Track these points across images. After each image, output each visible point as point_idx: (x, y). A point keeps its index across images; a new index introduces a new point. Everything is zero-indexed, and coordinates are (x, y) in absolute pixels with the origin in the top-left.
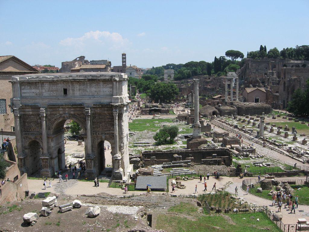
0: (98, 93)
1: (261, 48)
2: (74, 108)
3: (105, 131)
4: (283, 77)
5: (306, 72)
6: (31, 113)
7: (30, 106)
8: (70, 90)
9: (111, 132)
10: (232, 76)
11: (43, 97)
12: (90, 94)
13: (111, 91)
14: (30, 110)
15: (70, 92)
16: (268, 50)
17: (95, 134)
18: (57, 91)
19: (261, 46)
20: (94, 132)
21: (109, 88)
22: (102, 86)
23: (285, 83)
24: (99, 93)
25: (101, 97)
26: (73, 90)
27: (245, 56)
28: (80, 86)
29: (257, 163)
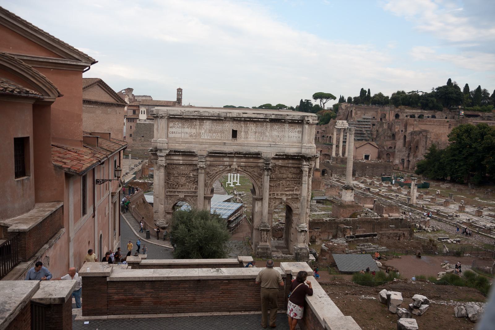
0: (281, 139)
1: (363, 92)
2: (245, 157)
3: (286, 191)
4: (404, 130)
6: (181, 162)
7: (182, 152)
8: (241, 132)
9: (295, 192)
10: (343, 125)
11: (201, 141)
12: (270, 140)
13: (299, 137)
14: (180, 158)
15: (241, 135)
16: (372, 95)
17: (272, 195)
18: (222, 132)
19: (362, 89)
20: (271, 193)
22: (287, 129)
23: (405, 137)
24: (282, 139)
25: (286, 144)
26: (246, 133)
27: (337, 101)
28: (256, 127)
29: (443, 239)
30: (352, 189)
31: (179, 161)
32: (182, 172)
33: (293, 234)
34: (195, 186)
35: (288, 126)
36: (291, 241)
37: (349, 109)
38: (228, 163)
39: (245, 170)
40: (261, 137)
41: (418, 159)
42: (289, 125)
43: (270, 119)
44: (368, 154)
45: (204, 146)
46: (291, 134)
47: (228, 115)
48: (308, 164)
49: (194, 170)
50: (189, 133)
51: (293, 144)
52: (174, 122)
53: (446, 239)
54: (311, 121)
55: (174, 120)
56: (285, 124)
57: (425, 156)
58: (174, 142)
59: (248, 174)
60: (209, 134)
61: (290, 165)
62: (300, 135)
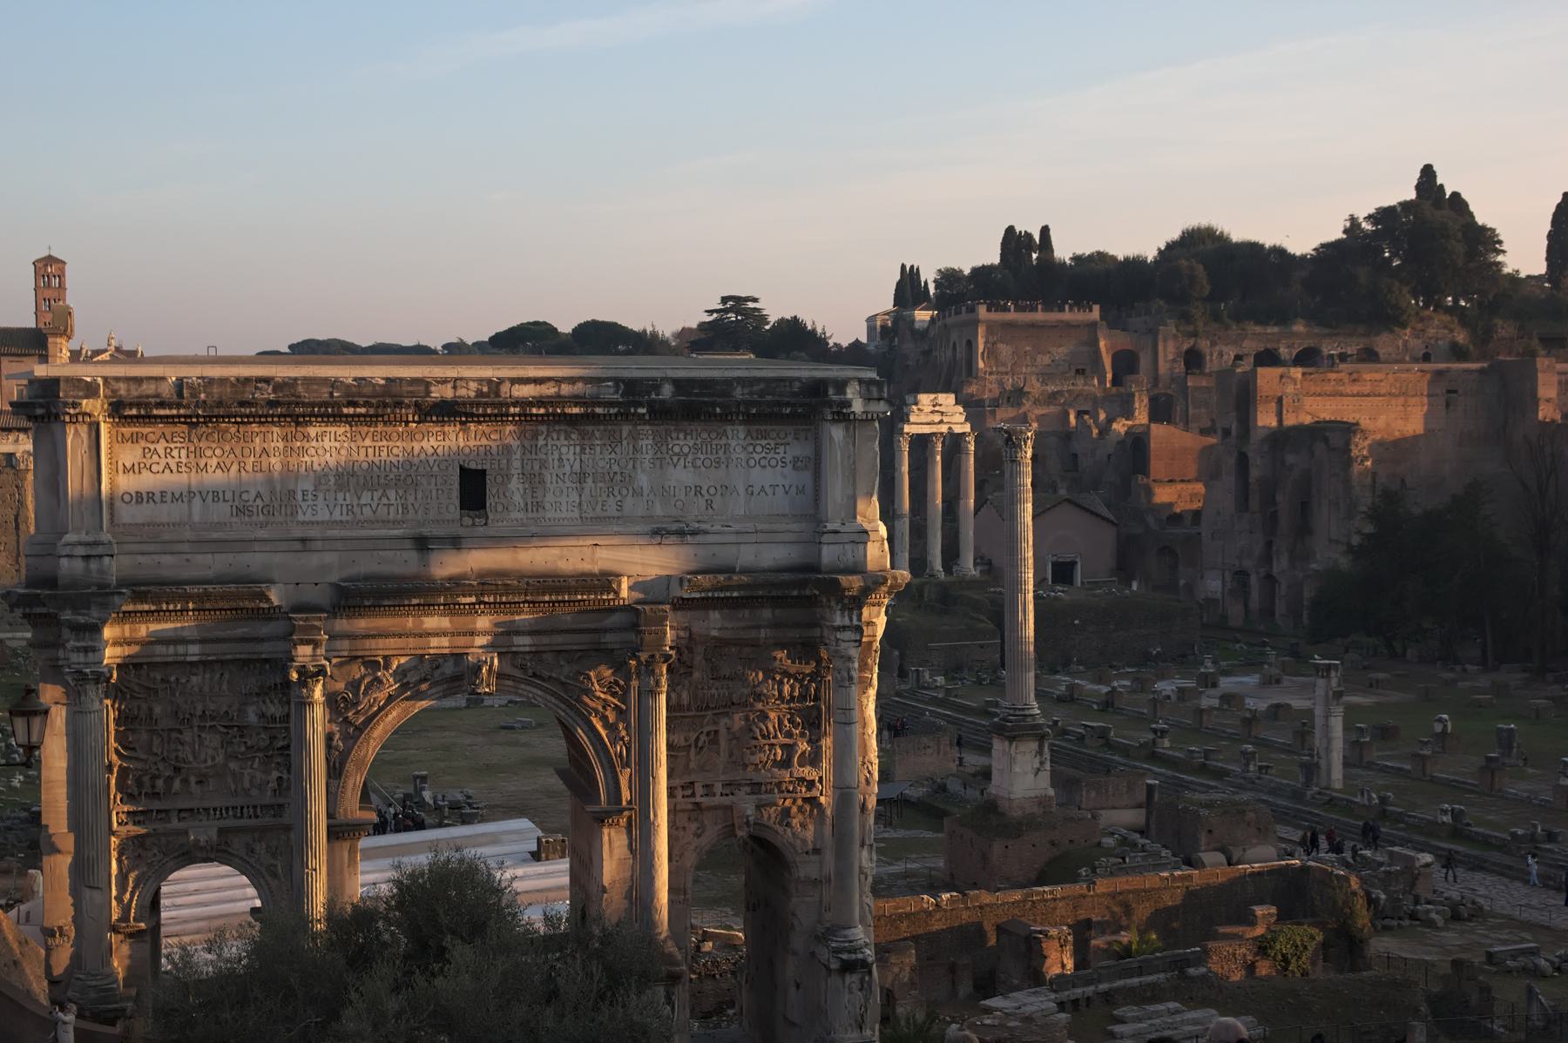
0: (709, 504)
1: (1014, 242)
5: (1358, 395)
8: (509, 477)
10: (937, 418)
12: (658, 510)
15: (509, 494)
17: (679, 793)
19: (1010, 230)
21: (790, 466)
22: (738, 454)
23: (1243, 461)
24: (717, 500)
25: (736, 527)
26: (534, 480)
28: (583, 450)
29: (1514, 955)
30: (1041, 738)
31: (181, 649)
32: (200, 707)
33: (798, 986)
34: (275, 774)
35: (742, 436)
36: (793, 1024)
37: (954, 336)
38: (445, 642)
39: (534, 675)
40: (612, 501)
41: (1314, 566)
42: (749, 433)
43: (651, 405)
44: (1068, 557)
45: (314, 560)
46: (762, 477)
47: (437, 393)
48: (855, 622)
49: (263, 692)
50: (229, 496)
51: (775, 527)
52: (143, 443)
53: (1523, 952)
54: (858, 406)
55: (146, 430)
56: (729, 428)
57: (1350, 549)
58: (152, 548)
59: (553, 694)
60: (340, 496)
61: (763, 633)
62: (806, 478)
